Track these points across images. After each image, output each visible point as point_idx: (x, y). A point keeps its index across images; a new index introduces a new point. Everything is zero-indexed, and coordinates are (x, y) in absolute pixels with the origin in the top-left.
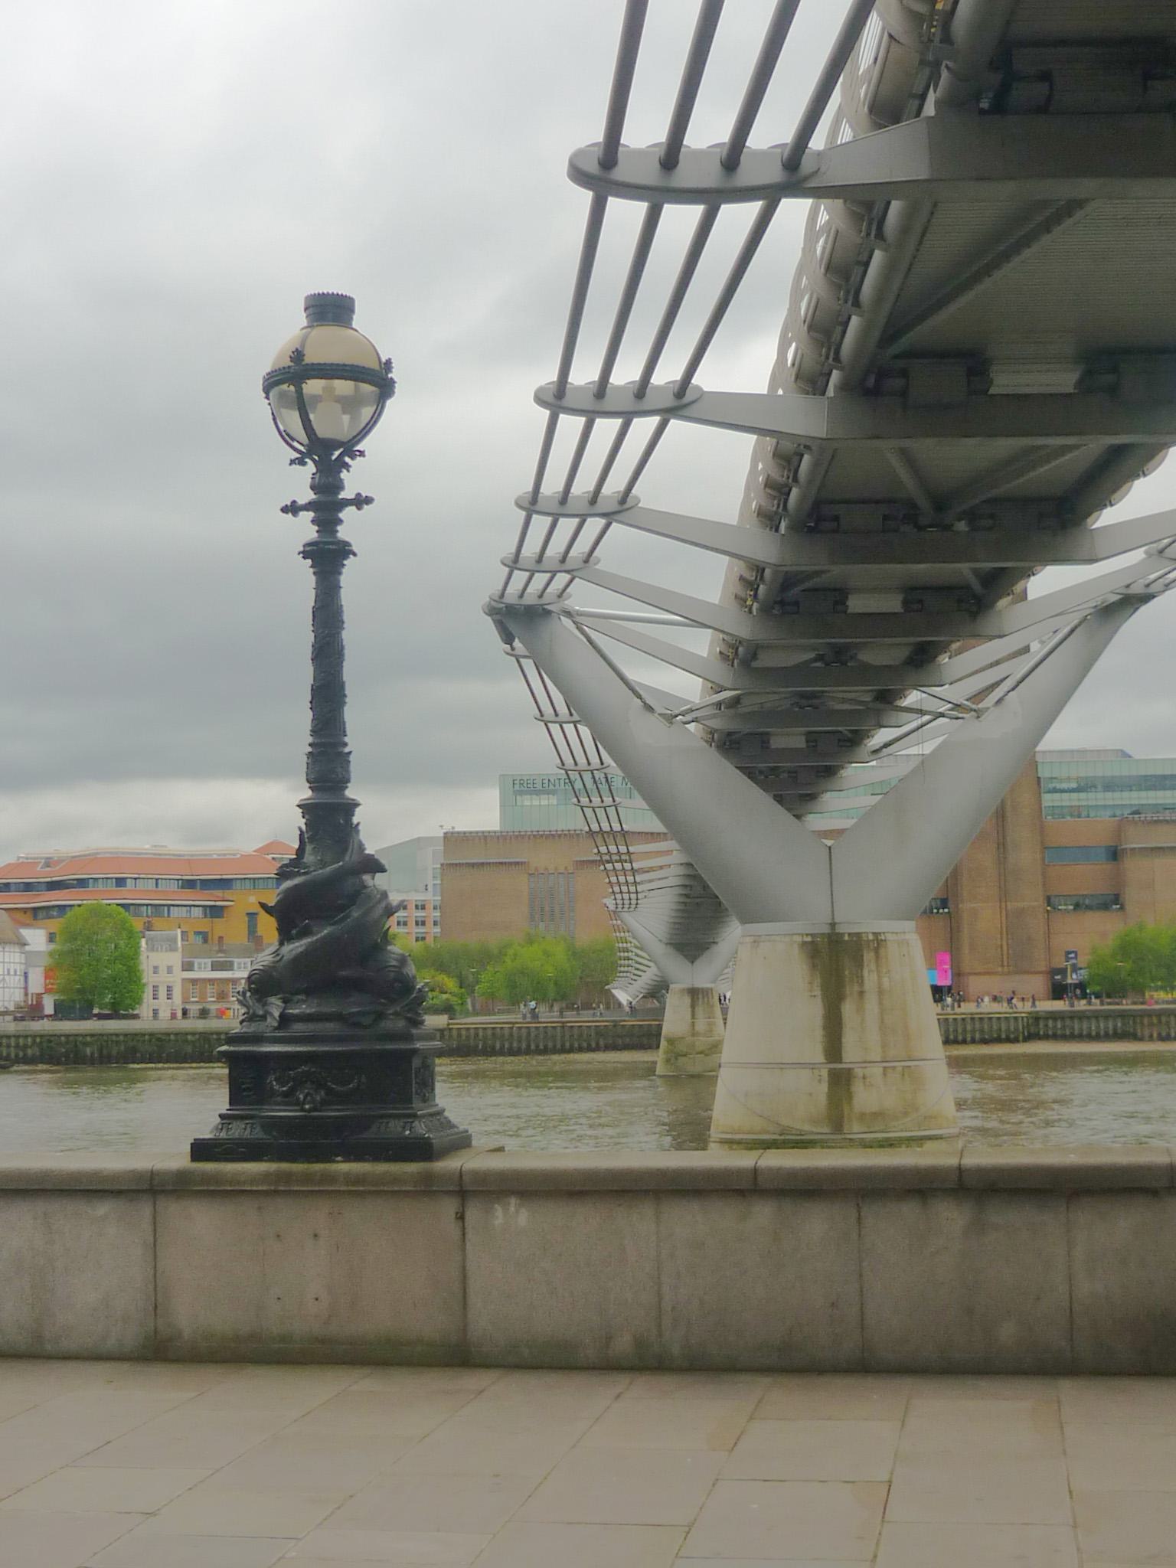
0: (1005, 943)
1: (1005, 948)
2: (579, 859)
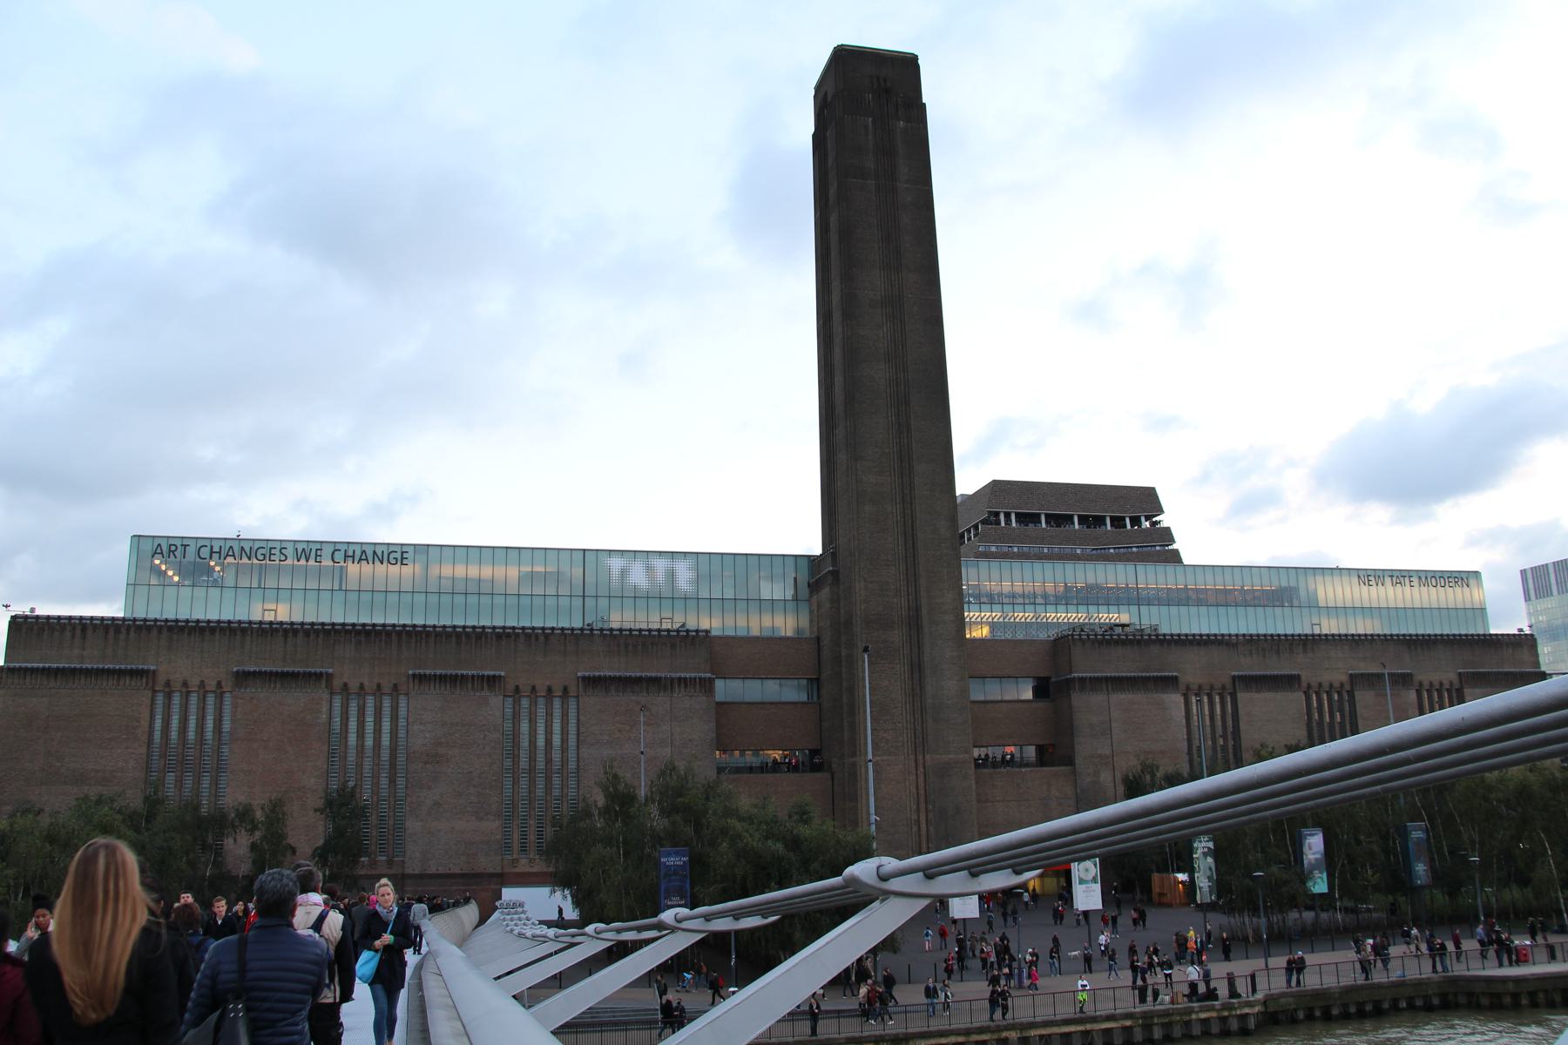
0: (923, 818)
1: (924, 826)
2: (240, 668)
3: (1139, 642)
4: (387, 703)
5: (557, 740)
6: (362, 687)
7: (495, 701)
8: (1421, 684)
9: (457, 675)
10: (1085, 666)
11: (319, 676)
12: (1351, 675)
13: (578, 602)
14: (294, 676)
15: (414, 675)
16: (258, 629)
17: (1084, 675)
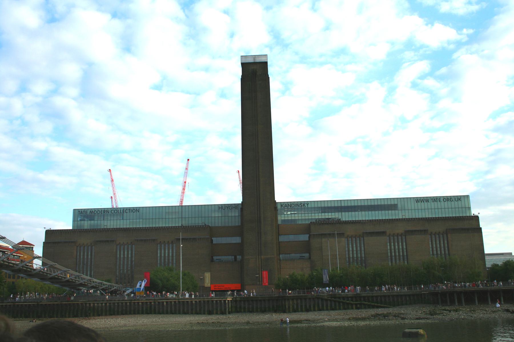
3: (332, 224)
4: (130, 246)
5: (171, 254)
6: (124, 243)
8: (431, 233)
9: (146, 240)
11: (113, 241)
12: (405, 231)
14: (108, 241)
15: (136, 240)
16: (99, 231)
17: (314, 233)
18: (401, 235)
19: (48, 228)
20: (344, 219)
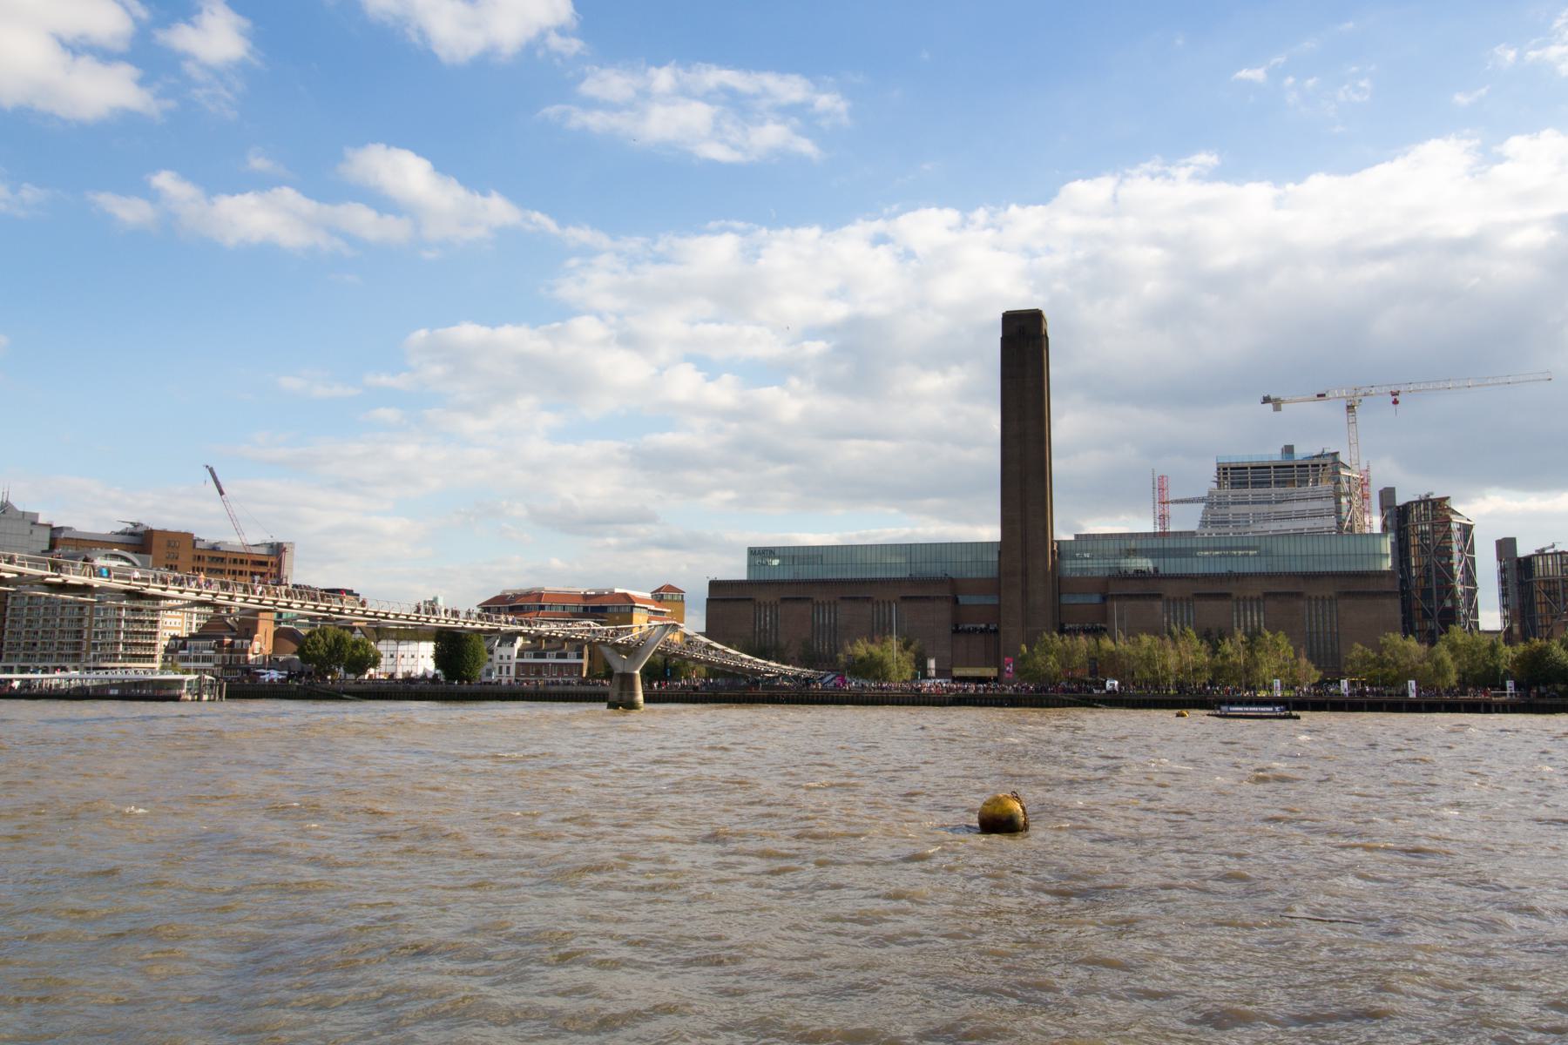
7: (870, 606)
10: (1114, 590)
11: (808, 599)
13: (908, 565)
14: (800, 599)
18: (1258, 599)
19: (712, 578)
20: (1167, 572)
